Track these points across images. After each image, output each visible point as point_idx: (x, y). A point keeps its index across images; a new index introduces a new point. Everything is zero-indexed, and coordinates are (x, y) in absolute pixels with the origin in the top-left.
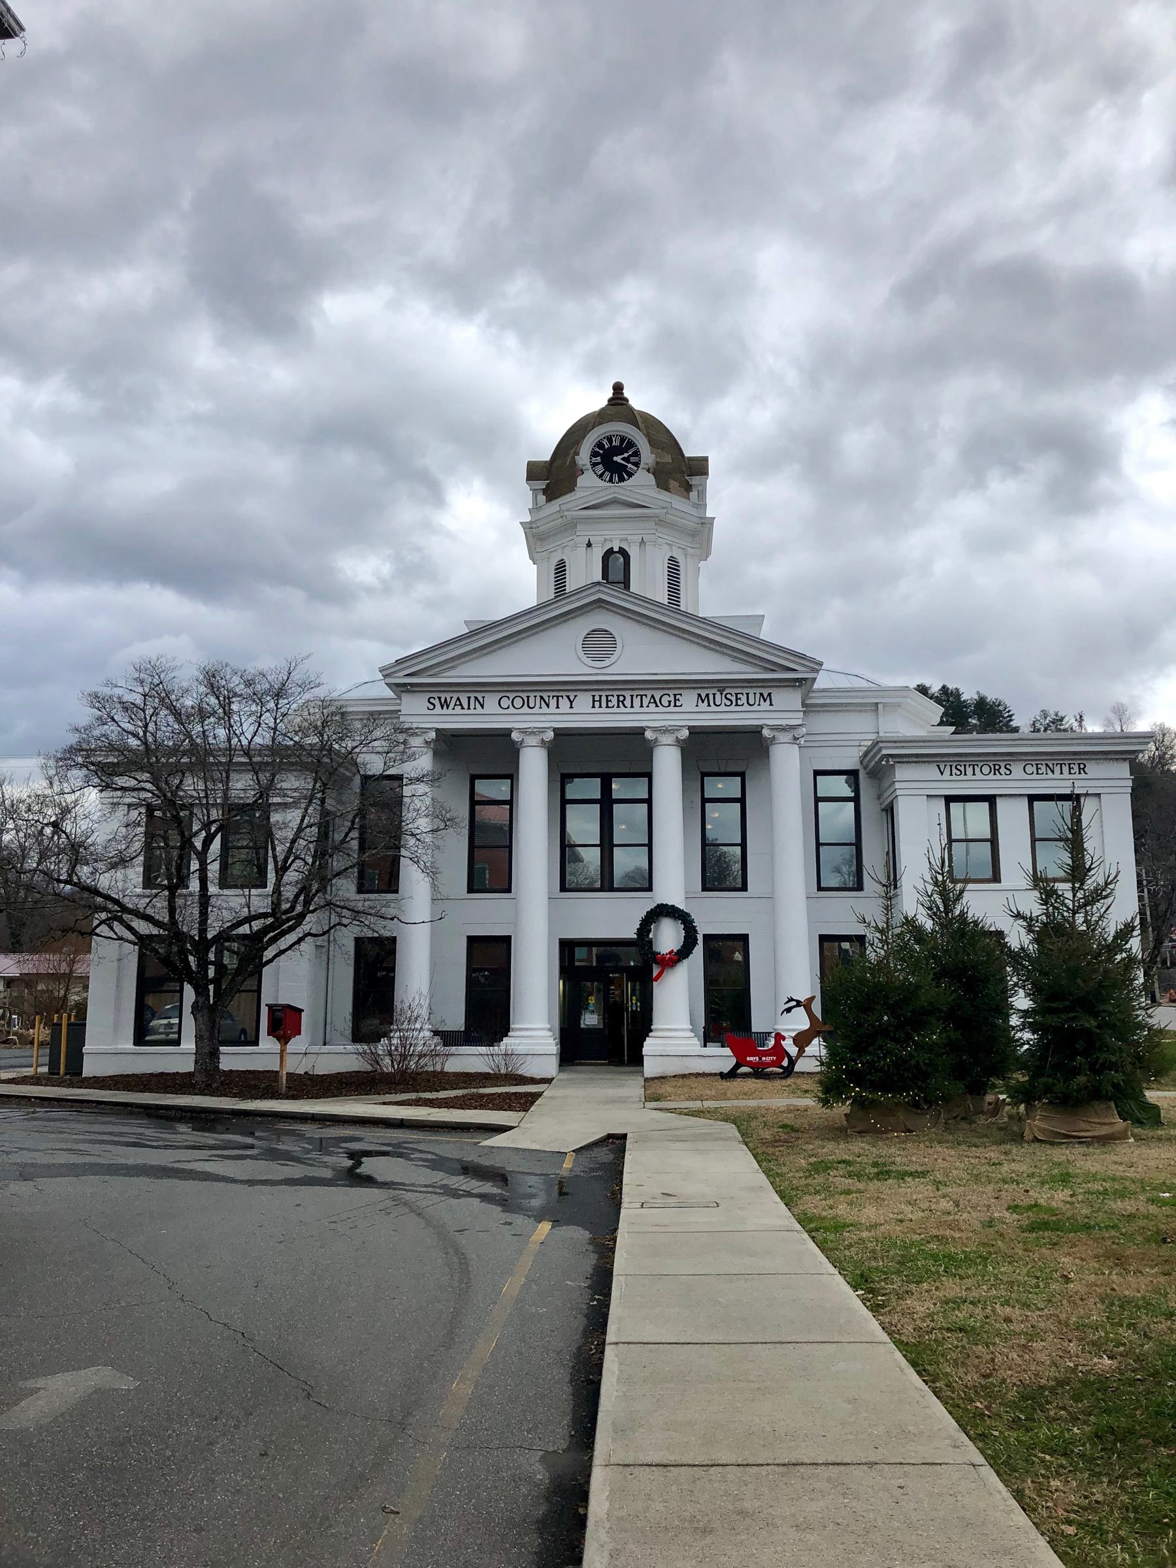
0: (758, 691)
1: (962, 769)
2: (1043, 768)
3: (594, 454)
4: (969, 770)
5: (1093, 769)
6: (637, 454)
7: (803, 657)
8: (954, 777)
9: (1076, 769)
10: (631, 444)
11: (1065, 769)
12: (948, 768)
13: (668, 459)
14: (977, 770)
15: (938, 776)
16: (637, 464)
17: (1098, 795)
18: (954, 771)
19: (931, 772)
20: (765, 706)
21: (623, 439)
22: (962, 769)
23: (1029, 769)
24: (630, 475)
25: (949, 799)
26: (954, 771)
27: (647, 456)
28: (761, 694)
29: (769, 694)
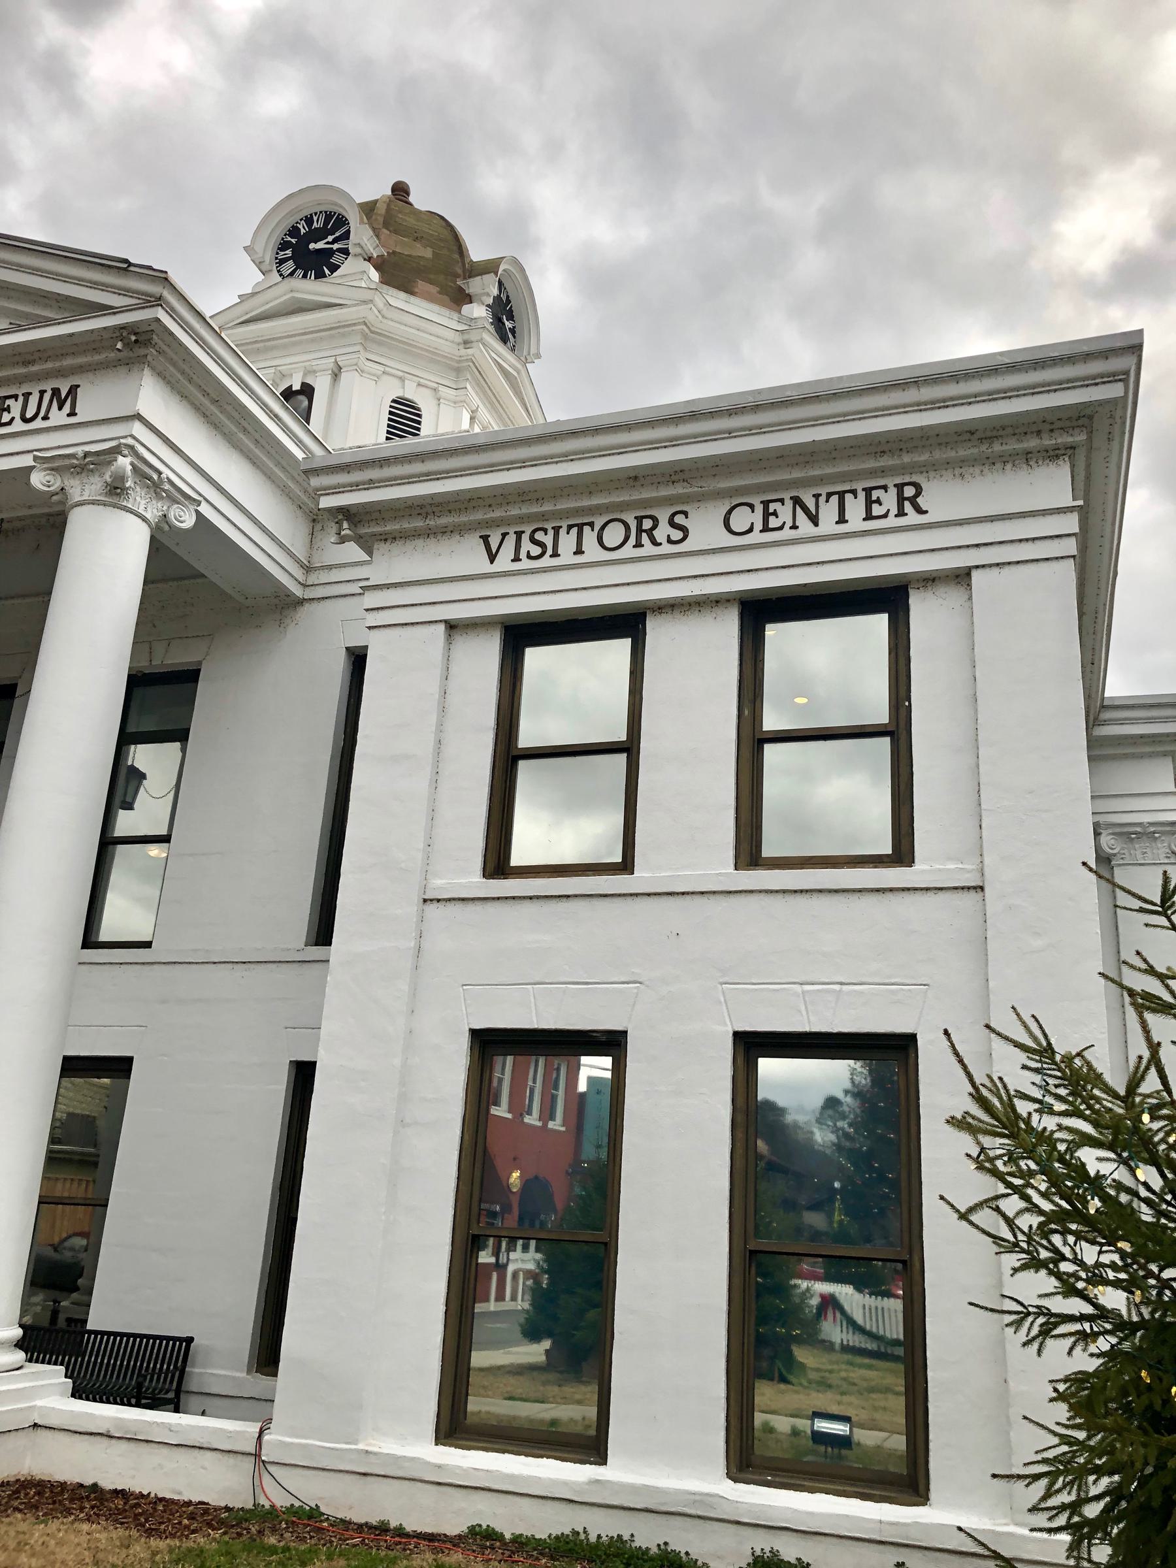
0: (48, 386)
1: (548, 540)
2: (785, 513)
3: (284, 246)
4: (567, 542)
5: (943, 498)
6: (346, 236)
7: (124, 266)
8: (525, 564)
9: (889, 500)
10: (342, 221)
11: (855, 508)
12: (511, 541)
13: (428, 253)
14: (590, 536)
15: (481, 564)
16: (346, 252)
17: (962, 577)
18: (527, 546)
19: (466, 556)
20: (58, 417)
21: (329, 216)
22: (548, 540)
23: (741, 519)
24: (334, 268)
25: (521, 635)
26: (527, 546)
27: (362, 236)
28: (56, 392)
29: (73, 390)
